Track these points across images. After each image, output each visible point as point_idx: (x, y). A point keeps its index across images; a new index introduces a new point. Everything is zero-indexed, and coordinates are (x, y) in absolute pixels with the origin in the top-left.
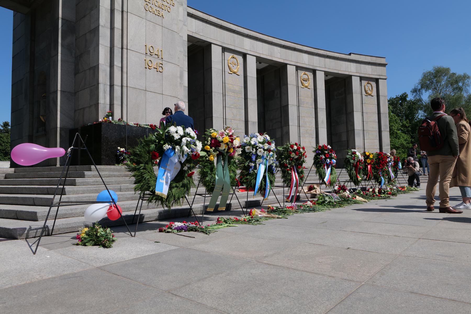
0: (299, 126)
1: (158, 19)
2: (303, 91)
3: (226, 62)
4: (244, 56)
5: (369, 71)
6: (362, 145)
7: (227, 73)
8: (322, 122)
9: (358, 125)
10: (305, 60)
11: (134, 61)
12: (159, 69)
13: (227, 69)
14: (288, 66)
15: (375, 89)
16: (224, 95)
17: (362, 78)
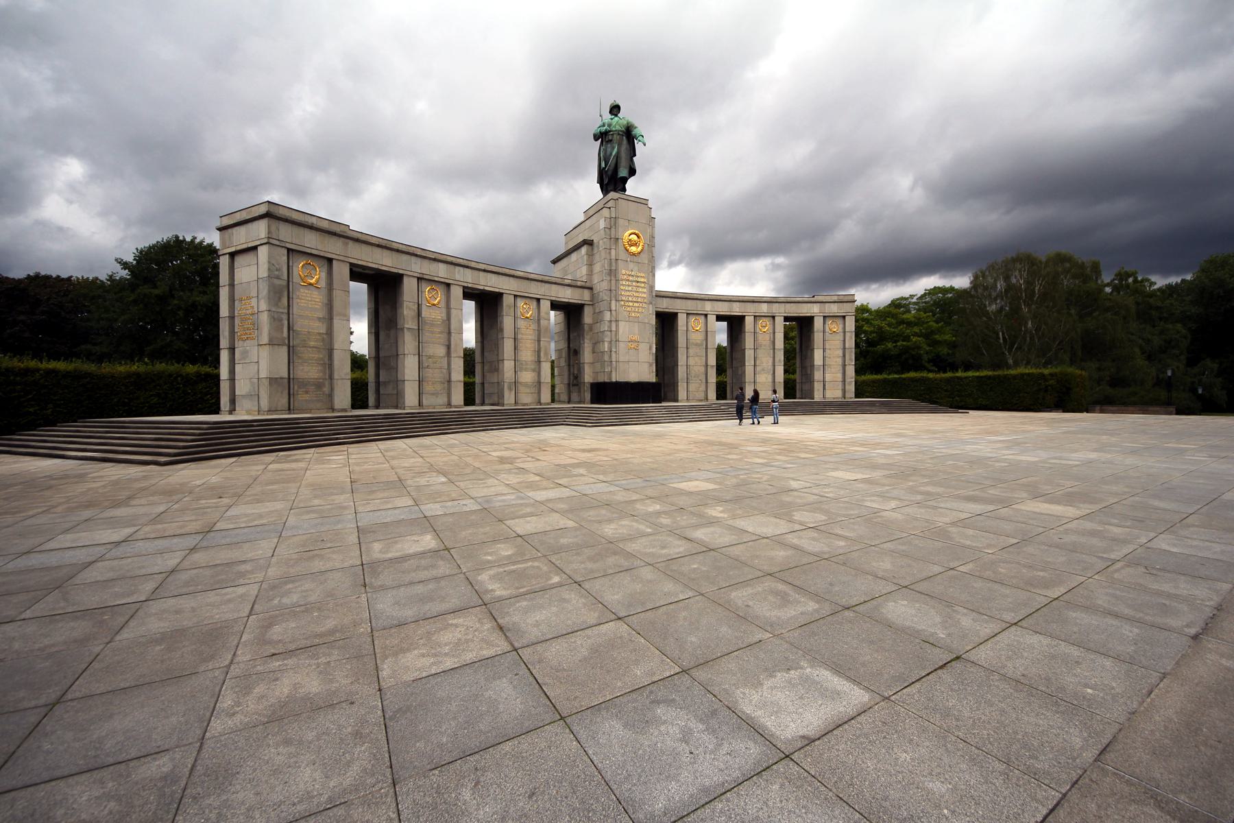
2: (760, 337)
4: (706, 315)
10: (764, 308)
11: (622, 345)
15: (841, 326)
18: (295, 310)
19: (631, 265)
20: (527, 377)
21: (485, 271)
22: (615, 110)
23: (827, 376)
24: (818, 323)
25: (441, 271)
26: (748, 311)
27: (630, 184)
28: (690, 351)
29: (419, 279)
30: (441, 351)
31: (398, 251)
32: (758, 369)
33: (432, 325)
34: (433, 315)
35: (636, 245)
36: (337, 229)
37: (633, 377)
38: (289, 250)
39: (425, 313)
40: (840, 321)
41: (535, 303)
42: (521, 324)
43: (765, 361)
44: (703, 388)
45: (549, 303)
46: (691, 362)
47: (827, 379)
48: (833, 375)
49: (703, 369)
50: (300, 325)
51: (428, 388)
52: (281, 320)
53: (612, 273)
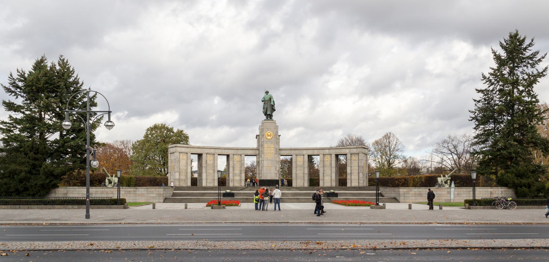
0: (324, 174)
5: (354, 151)
9: (349, 171)
10: (327, 152)
11: (265, 168)
20: (237, 178)
22: (267, 93)
25: (212, 151)
27: (273, 114)
30: (212, 172)
32: (325, 174)
34: (210, 162)
35: (270, 136)
37: (269, 178)
39: (208, 162)
40: (357, 156)
42: (235, 163)
43: (328, 171)
44: (303, 181)
46: (298, 172)
48: (355, 177)
49: (302, 175)
50: (181, 168)
51: (208, 181)
53: (262, 146)
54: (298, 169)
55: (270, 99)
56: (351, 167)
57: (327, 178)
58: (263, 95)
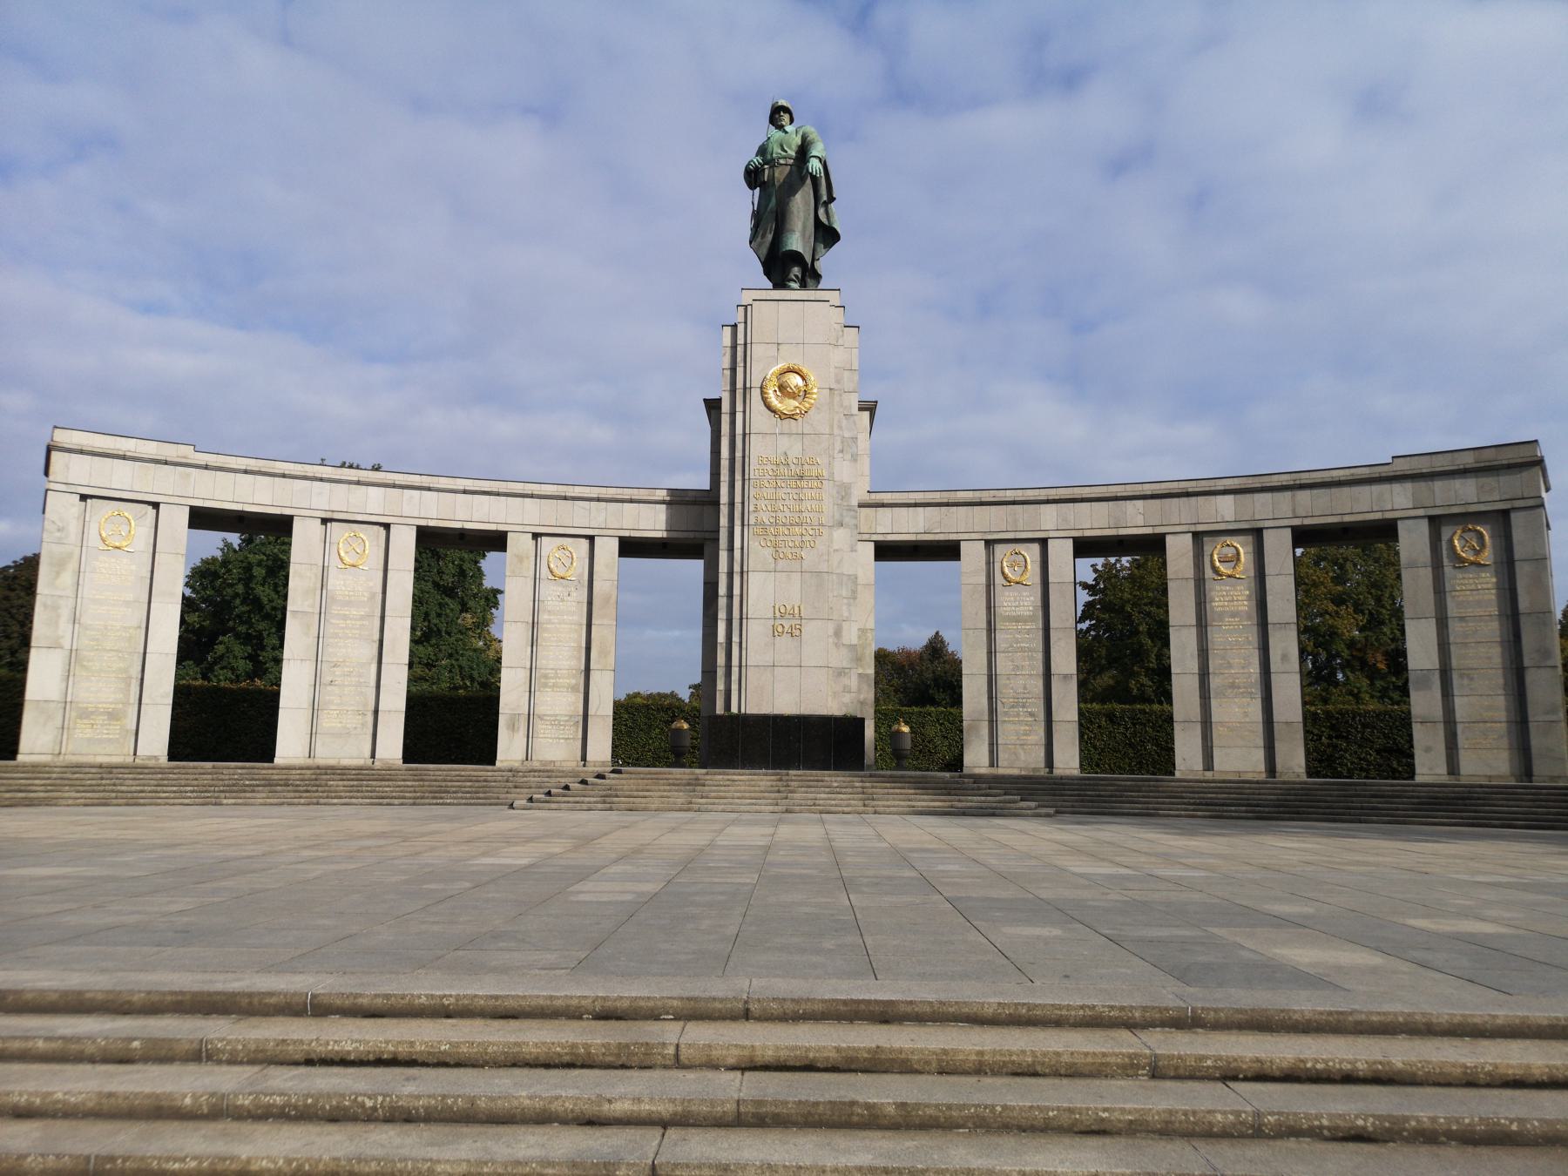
0: (1204, 675)
1: (796, 565)
3: (997, 566)
5: (1466, 493)
6: (1438, 712)
7: (999, 589)
8: (1285, 657)
10: (1225, 510)
12: (795, 633)
13: (999, 579)
14: (1169, 539)
16: (991, 629)
17: (1435, 522)
18: (86, 591)
19: (784, 443)
20: (560, 702)
21: (465, 492)
23: (1459, 702)
24: (1413, 543)
25: (373, 502)
26: (1174, 521)
27: (827, 262)
28: (1000, 637)
29: (325, 521)
31: (284, 476)
32: (1215, 682)
33: (349, 604)
36: (170, 452)
38: (84, 498)
39: (334, 582)
41: (585, 543)
42: (549, 591)
45: (615, 544)
46: (1003, 665)
47: (1460, 715)
49: (1039, 684)
51: (327, 722)
52: (55, 608)
54: (1002, 639)
55: (803, 151)
56: (1442, 623)
57: (1237, 712)
58: (761, 131)
